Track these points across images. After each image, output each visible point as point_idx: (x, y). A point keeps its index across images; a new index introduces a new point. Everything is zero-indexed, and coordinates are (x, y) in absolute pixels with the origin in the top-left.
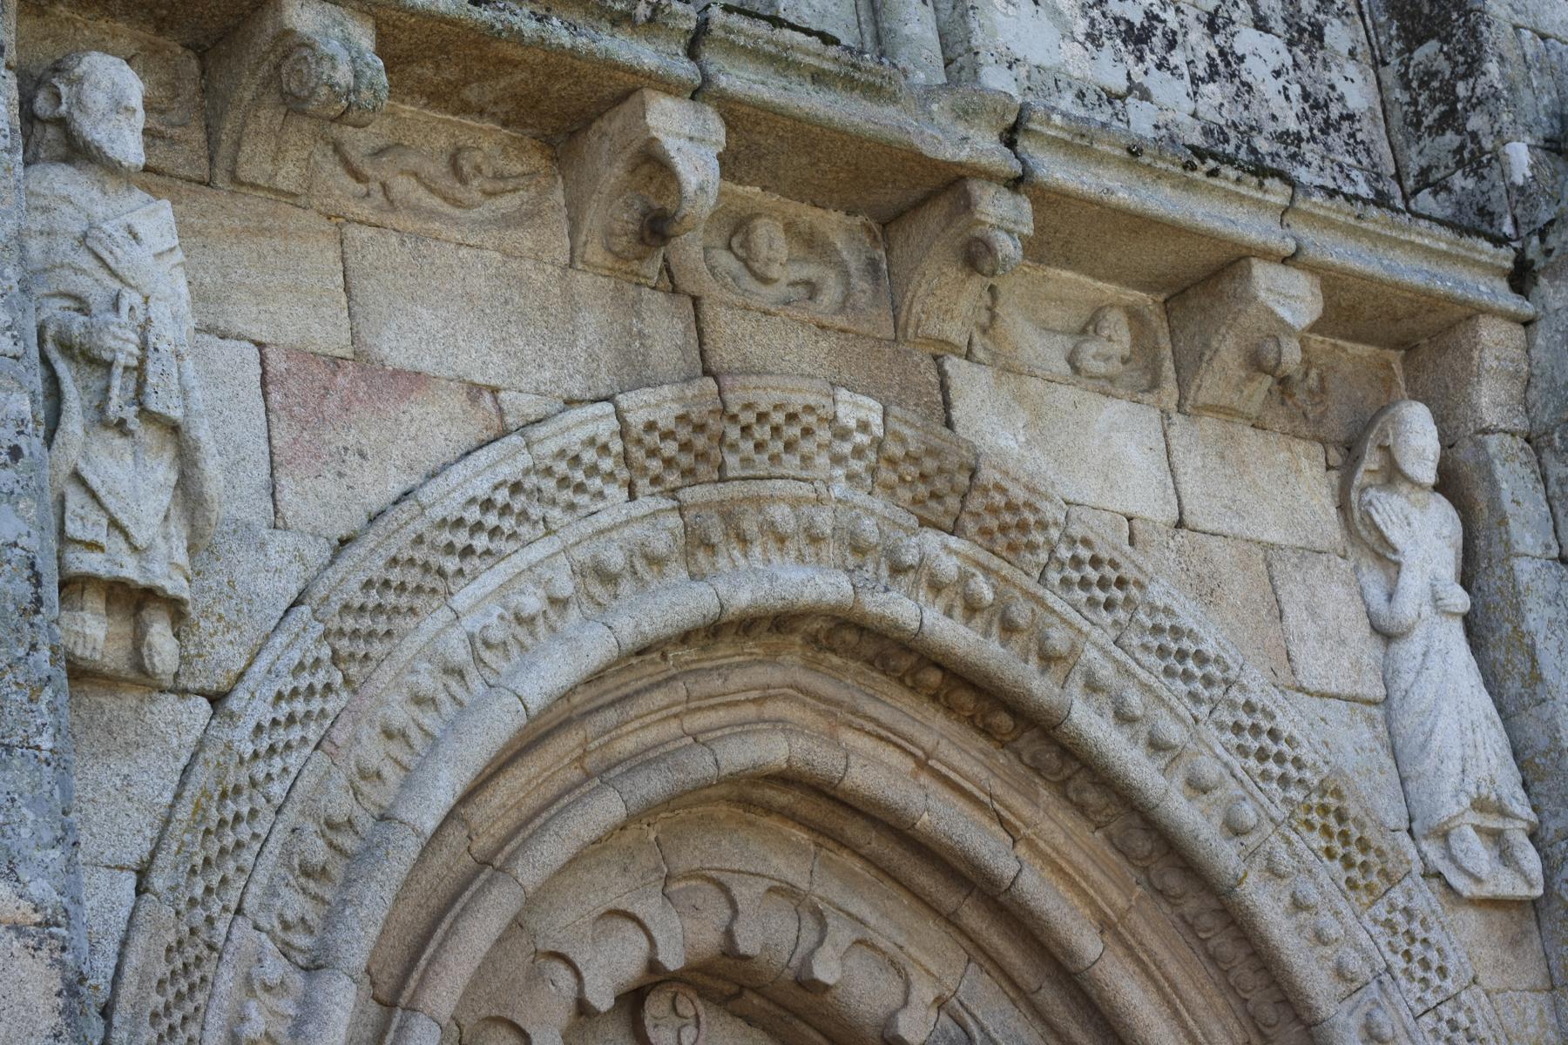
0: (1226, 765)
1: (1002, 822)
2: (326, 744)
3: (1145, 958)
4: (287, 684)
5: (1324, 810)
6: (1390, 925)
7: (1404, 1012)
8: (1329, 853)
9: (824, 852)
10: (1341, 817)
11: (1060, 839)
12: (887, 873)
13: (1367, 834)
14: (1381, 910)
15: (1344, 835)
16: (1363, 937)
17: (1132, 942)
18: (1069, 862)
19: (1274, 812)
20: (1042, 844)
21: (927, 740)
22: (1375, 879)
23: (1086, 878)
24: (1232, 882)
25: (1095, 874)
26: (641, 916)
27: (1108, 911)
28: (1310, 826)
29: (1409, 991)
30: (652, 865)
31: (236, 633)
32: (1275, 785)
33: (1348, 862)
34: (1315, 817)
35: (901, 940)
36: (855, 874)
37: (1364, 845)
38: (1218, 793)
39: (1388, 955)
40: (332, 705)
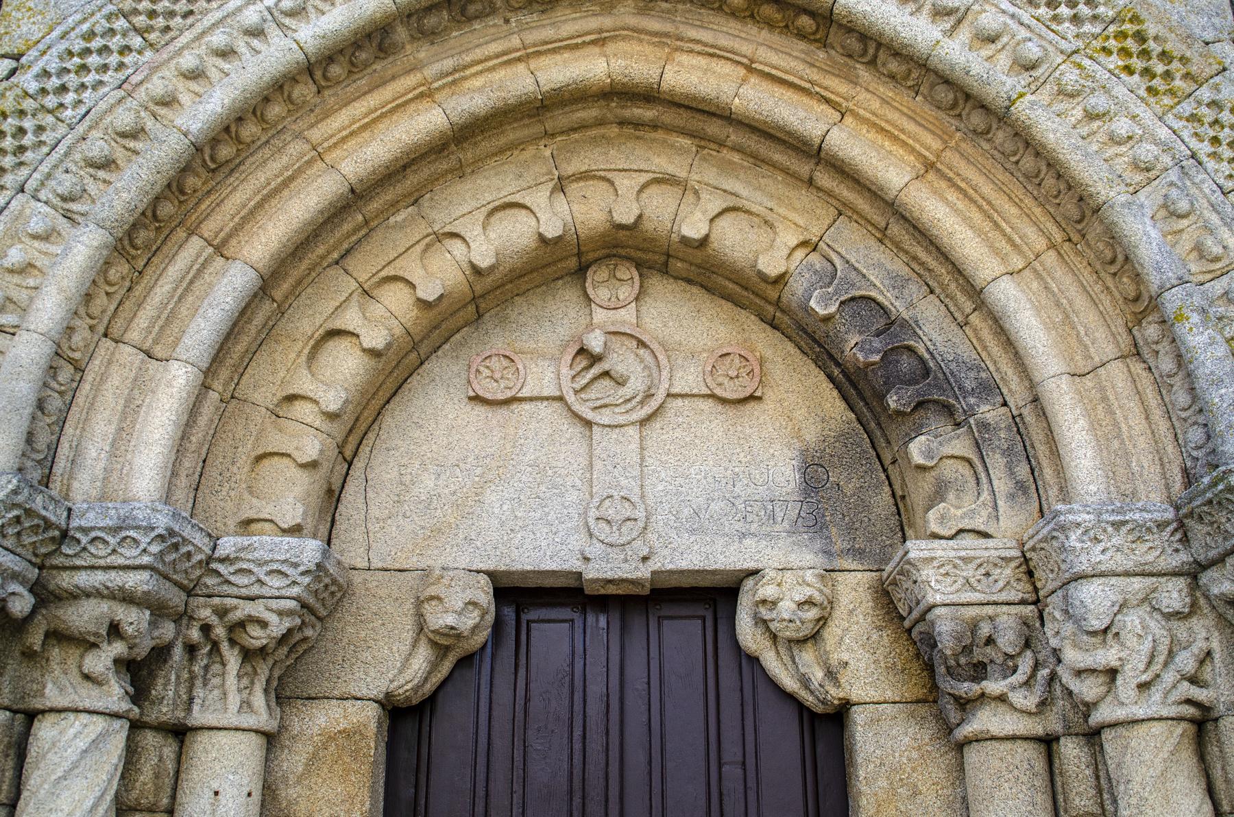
0: (1013, 16)
1: (828, 101)
2: (125, 86)
3: (963, 185)
4: (78, 45)
5: (1122, 35)
6: (1193, 118)
7: (1208, 186)
8: (1129, 70)
9: (706, 151)
10: (1140, 37)
11: (875, 104)
12: (758, 160)
13: (1168, 47)
14: (1187, 108)
15: (1145, 54)
16: (1163, 133)
17: (951, 175)
18: (887, 121)
19: (1064, 45)
20: (862, 112)
21: (746, 49)
22: (1178, 83)
23: (902, 131)
24: (1007, 103)
25: (911, 127)
26: (529, 205)
27: (927, 154)
28: (1106, 51)
29: (1217, 171)
30: (544, 170)
31: (39, 17)
32: (1067, 24)
33: (1147, 73)
34: (1112, 44)
35: (769, 205)
36: (735, 163)
37: (1165, 56)
38: (1005, 39)
39: (1193, 143)
40: (128, 60)
